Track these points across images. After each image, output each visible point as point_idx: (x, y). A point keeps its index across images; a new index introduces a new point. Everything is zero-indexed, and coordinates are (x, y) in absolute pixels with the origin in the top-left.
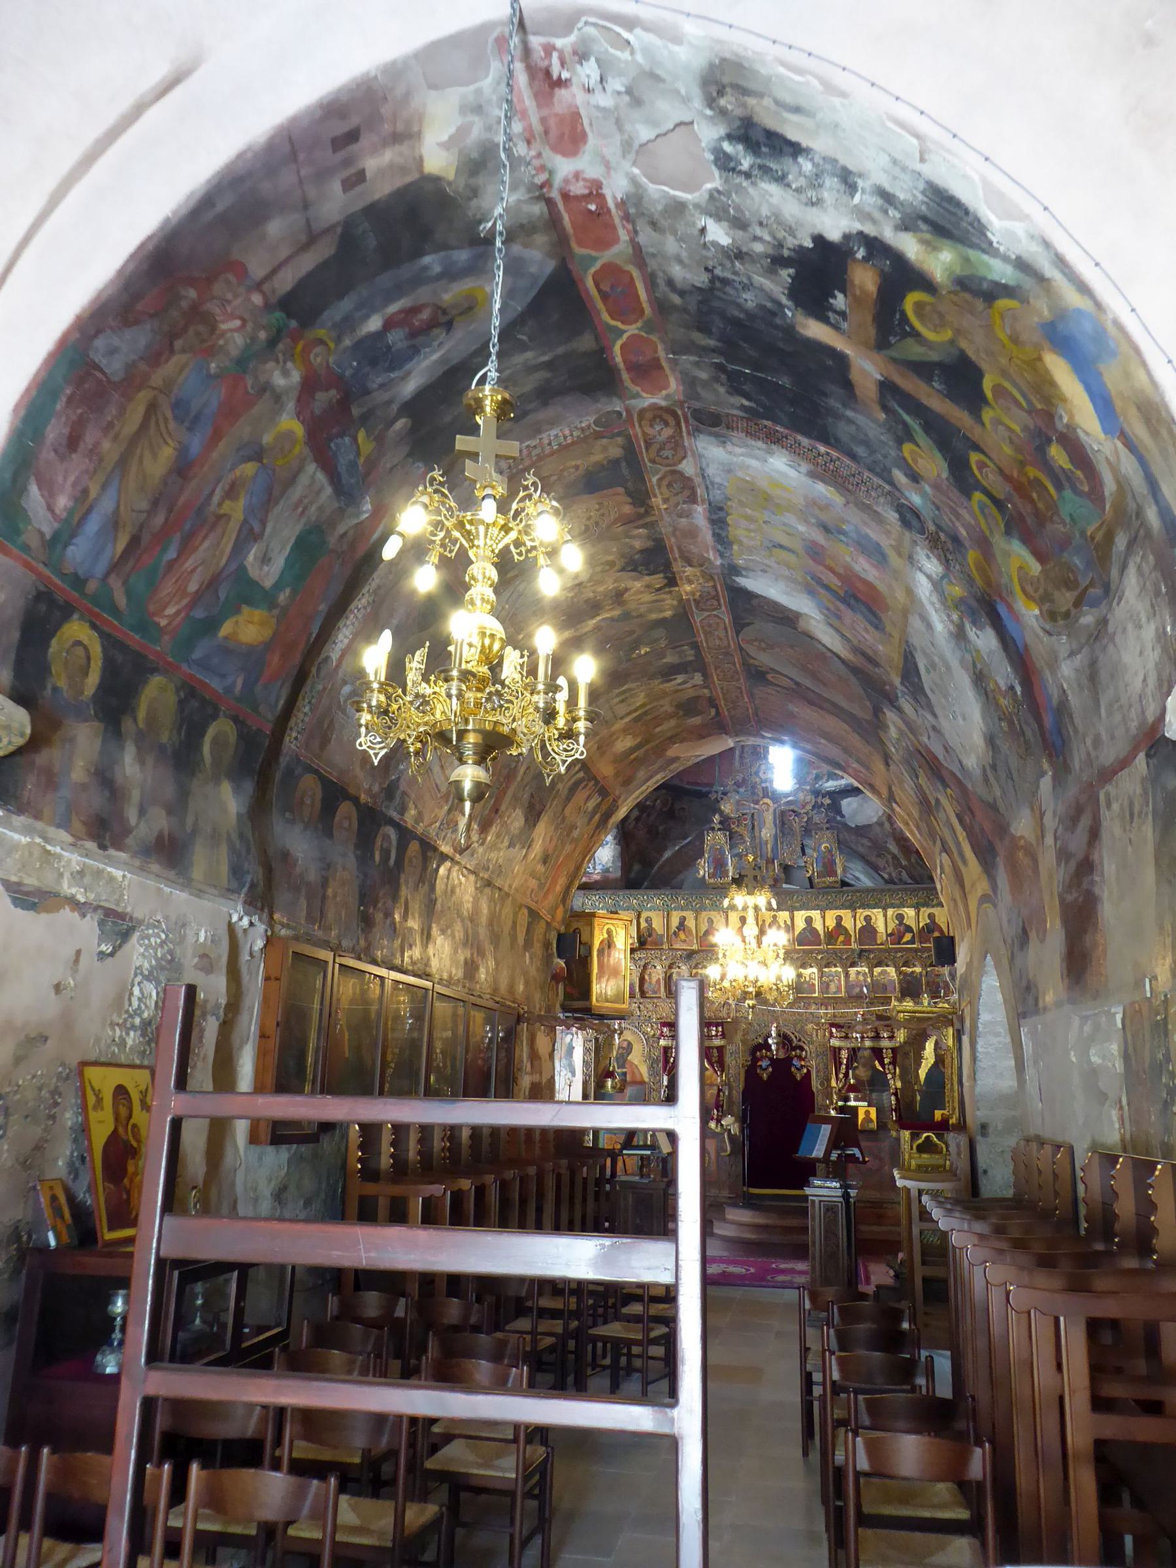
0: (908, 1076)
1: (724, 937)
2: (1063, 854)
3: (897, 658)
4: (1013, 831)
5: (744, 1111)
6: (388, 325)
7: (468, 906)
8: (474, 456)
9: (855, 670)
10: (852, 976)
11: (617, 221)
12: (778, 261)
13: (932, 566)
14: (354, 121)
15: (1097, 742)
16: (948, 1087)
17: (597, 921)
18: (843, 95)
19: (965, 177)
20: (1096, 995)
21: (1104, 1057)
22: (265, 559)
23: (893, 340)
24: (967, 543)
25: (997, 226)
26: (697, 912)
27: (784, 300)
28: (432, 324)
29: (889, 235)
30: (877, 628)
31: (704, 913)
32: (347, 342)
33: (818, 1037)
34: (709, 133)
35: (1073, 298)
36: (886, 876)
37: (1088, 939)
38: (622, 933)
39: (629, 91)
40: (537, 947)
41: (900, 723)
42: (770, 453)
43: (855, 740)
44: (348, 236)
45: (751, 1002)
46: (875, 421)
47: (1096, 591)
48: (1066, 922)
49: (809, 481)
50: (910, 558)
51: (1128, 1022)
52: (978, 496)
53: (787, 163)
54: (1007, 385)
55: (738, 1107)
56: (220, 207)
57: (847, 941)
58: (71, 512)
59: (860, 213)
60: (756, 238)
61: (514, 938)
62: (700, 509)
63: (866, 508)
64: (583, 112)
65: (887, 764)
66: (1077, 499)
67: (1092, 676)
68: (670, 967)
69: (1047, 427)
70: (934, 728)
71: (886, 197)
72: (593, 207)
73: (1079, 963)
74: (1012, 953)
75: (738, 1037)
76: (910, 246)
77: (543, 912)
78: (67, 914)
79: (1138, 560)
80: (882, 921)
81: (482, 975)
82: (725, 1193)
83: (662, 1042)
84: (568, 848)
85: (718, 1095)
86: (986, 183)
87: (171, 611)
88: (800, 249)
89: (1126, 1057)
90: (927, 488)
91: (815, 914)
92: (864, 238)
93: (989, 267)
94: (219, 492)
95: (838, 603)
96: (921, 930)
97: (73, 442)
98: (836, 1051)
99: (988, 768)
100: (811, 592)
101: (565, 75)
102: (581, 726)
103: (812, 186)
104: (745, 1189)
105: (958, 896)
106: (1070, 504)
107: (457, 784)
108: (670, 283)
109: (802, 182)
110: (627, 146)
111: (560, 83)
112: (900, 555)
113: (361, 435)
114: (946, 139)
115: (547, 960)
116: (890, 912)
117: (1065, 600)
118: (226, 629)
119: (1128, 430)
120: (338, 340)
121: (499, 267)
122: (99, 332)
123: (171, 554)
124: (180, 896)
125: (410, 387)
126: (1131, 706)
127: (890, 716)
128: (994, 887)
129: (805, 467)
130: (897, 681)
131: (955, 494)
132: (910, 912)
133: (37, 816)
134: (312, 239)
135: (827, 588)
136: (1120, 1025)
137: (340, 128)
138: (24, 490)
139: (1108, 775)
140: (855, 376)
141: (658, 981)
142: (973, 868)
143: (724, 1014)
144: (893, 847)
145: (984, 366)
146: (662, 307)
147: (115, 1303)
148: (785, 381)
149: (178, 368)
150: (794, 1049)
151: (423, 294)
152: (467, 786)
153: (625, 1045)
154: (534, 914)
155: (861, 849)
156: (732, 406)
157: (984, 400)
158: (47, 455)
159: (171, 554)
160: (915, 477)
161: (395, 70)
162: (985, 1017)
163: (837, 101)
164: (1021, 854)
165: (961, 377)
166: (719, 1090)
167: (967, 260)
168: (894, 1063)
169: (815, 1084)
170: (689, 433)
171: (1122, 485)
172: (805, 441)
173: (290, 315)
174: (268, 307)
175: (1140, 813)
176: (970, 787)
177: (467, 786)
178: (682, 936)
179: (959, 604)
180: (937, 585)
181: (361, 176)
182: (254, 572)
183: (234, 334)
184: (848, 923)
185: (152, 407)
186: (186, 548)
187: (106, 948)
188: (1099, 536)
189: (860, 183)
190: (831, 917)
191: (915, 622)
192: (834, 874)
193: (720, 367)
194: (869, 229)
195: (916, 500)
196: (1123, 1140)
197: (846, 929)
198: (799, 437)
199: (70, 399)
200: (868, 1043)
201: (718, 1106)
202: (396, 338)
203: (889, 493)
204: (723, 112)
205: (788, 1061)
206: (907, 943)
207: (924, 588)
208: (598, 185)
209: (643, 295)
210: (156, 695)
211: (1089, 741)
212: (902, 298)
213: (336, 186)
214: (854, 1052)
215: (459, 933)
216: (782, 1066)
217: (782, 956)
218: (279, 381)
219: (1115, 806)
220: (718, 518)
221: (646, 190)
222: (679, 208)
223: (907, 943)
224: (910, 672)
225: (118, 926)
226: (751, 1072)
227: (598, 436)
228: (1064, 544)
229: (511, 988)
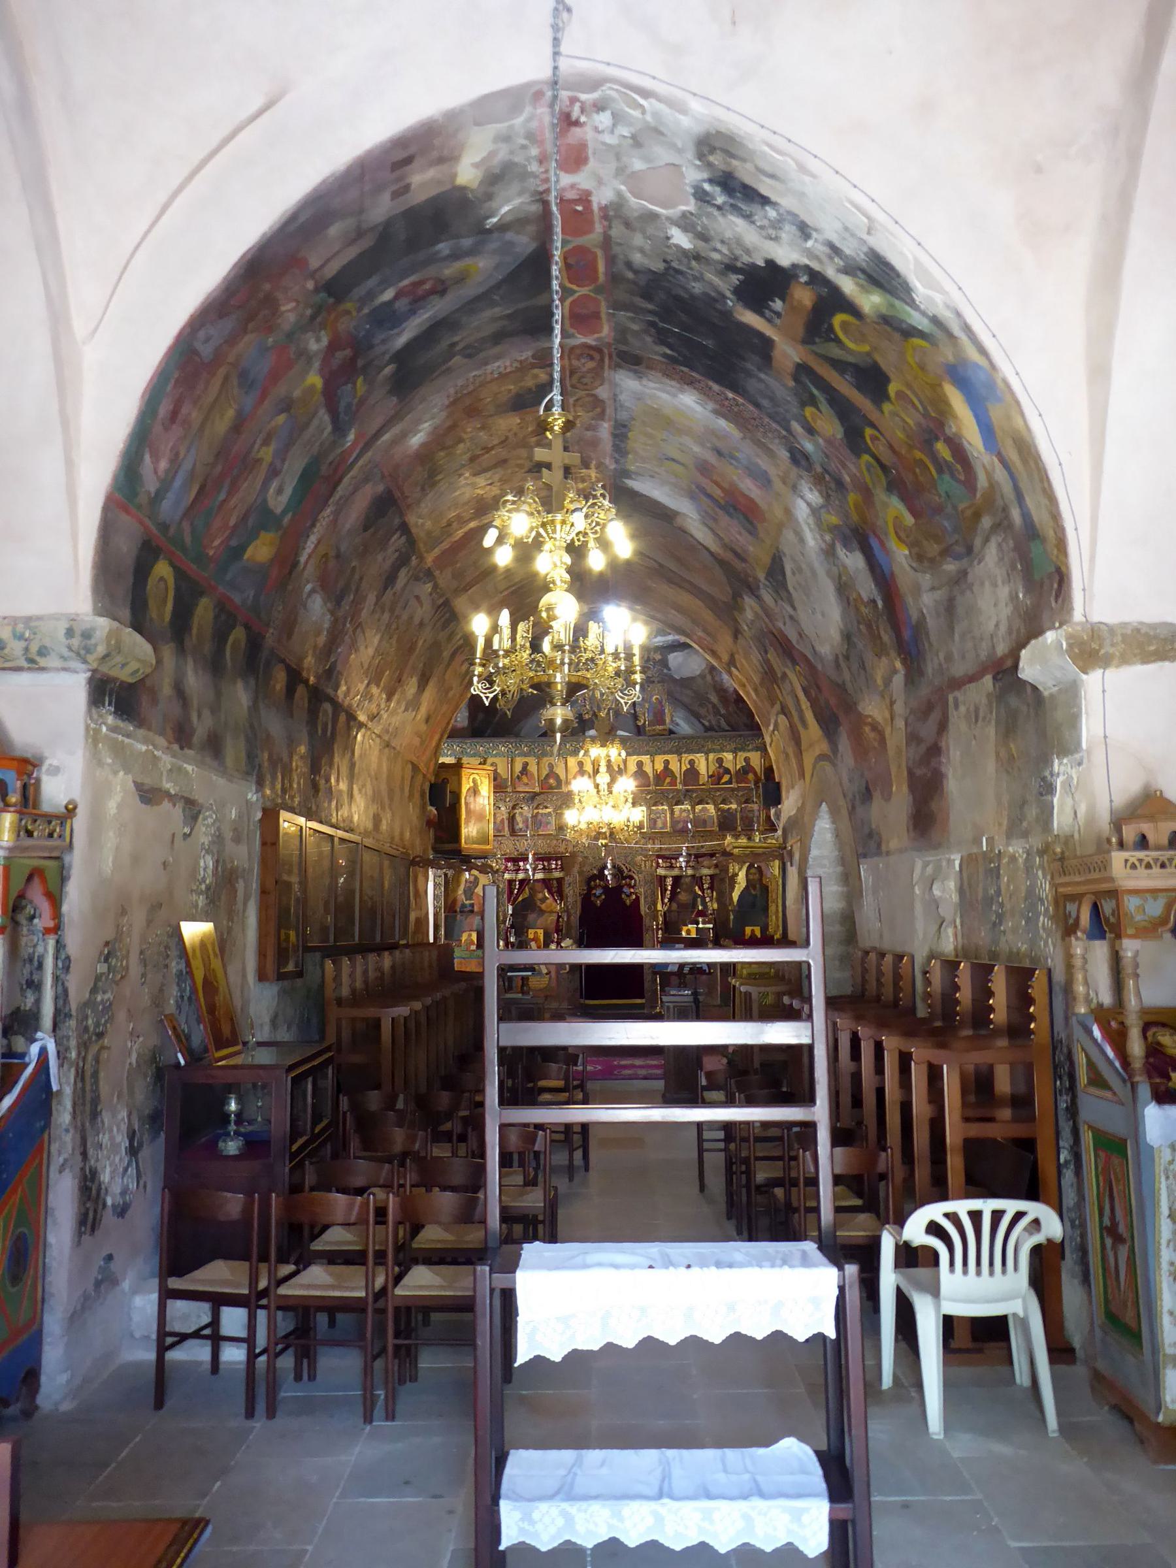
0: (724, 898)
1: (580, 785)
2: (913, 738)
3: (766, 560)
4: (860, 709)
5: (582, 935)
7: (374, 766)
8: (549, 466)
9: (722, 563)
10: (677, 813)
11: (596, 218)
12: (730, 267)
13: (814, 497)
14: (412, 150)
15: (949, 658)
16: (772, 908)
17: (464, 772)
18: (814, 176)
19: (901, 253)
20: (937, 846)
21: (943, 891)
22: (280, 491)
23: (817, 340)
24: (850, 487)
25: (921, 291)
26: (539, 759)
27: (728, 294)
28: (432, 292)
29: (830, 272)
30: (751, 533)
31: (545, 759)
32: (366, 311)
33: (646, 866)
34: (694, 175)
35: (973, 355)
36: (707, 724)
37: (934, 805)
38: (486, 781)
39: (634, 137)
40: (417, 795)
41: (758, 608)
42: (682, 391)
43: (708, 616)
44: (385, 233)
45: (604, 842)
46: (784, 385)
47: (959, 549)
48: (912, 788)
49: (712, 416)
50: (794, 488)
51: (964, 867)
52: (866, 457)
53: (755, 208)
54: (908, 392)
55: (575, 932)
56: (302, 219)
57: (673, 783)
58: (167, 471)
59: (809, 253)
60: (715, 250)
61: (402, 790)
62: (606, 425)
63: (759, 444)
64: (591, 145)
65: (736, 637)
66: (954, 483)
67: (949, 608)
68: (514, 808)
69: (935, 426)
70: (791, 617)
71: (835, 250)
72: (579, 208)
73: (926, 820)
74: (854, 807)
75: (576, 869)
76: (847, 285)
77: (422, 766)
78: (166, 805)
79: (1000, 539)
80: (703, 764)
81: (384, 826)
82: (565, 1005)
83: (507, 876)
84: (445, 708)
85: (558, 921)
86: (916, 260)
87: (216, 543)
88: (754, 266)
89: (961, 891)
90: (821, 441)
91: (646, 759)
92: (808, 270)
93: (910, 315)
94: (259, 442)
95: (718, 510)
96: (737, 772)
97: (174, 415)
98: (662, 879)
99: (841, 657)
100: (692, 497)
101: (583, 119)
102: (638, 677)
103: (775, 228)
104: (582, 1001)
105: (790, 751)
106: (946, 483)
107: (551, 722)
108: (629, 265)
109: (766, 222)
110: (620, 171)
111: (577, 123)
112: (784, 483)
113: (360, 380)
114: (891, 226)
115: (423, 807)
116: (711, 756)
117: (933, 549)
119: (1004, 453)
120: (359, 310)
121: (557, 307)
122: (202, 325)
123: (222, 496)
124: (221, 781)
125: (402, 340)
126: (982, 639)
127: (749, 602)
128: (835, 750)
129: (711, 405)
130: (761, 576)
131: (847, 452)
132: (728, 756)
133: (149, 729)
134: (360, 234)
135: (710, 496)
136: (957, 868)
137: (401, 155)
138: (142, 459)
139: (957, 684)
140: (776, 354)
141: (502, 821)
142: (813, 730)
143: (562, 850)
144: (714, 698)
145: (892, 376)
146: (615, 279)
147: (229, 1104)
148: (709, 343)
149: (248, 344)
150: (625, 878)
151: (431, 271)
152: (559, 721)
153: (472, 879)
154: (415, 768)
155: (686, 700)
156: (656, 353)
157: (888, 398)
158: (158, 428)
159: (222, 496)
160: (811, 431)
161: (452, 116)
162: (814, 852)
163: (807, 179)
164: (867, 729)
165: (873, 379)
166: (559, 917)
167: (892, 306)
168: (711, 888)
169: (644, 909)
170: (610, 367)
171: (993, 486)
172: (716, 387)
173: (330, 295)
174: (317, 290)
175: (984, 718)
176: (819, 667)
177: (559, 721)
178: (525, 779)
179: (832, 529)
180: (815, 511)
181: (407, 188)
182: (271, 503)
183: (289, 313)
184: (674, 766)
185: (226, 378)
186: (234, 488)
187: (187, 830)
188: (969, 513)
189: (814, 234)
190: (659, 761)
191: (789, 535)
192: (663, 722)
193: (652, 324)
194: (815, 266)
195: (809, 447)
196: (956, 949)
197: (672, 772)
198: (711, 383)
199: (177, 381)
200: (690, 872)
201: (558, 930)
202: (402, 305)
203: (785, 437)
204: (710, 165)
205: (618, 889)
206: (726, 783)
207: (802, 511)
208: (588, 193)
209: (601, 268)
210: (204, 612)
211: (942, 656)
212: (832, 315)
213: (386, 197)
214: (677, 880)
215: (369, 789)
216: (614, 894)
217: (630, 800)
218: (314, 346)
219: (962, 709)
220: (621, 433)
221: (627, 201)
222: (654, 216)
223: (726, 783)
224: (776, 571)
225: (192, 809)
226: (587, 899)
227: (533, 366)
228: (939, 510)
229: (402, 834)
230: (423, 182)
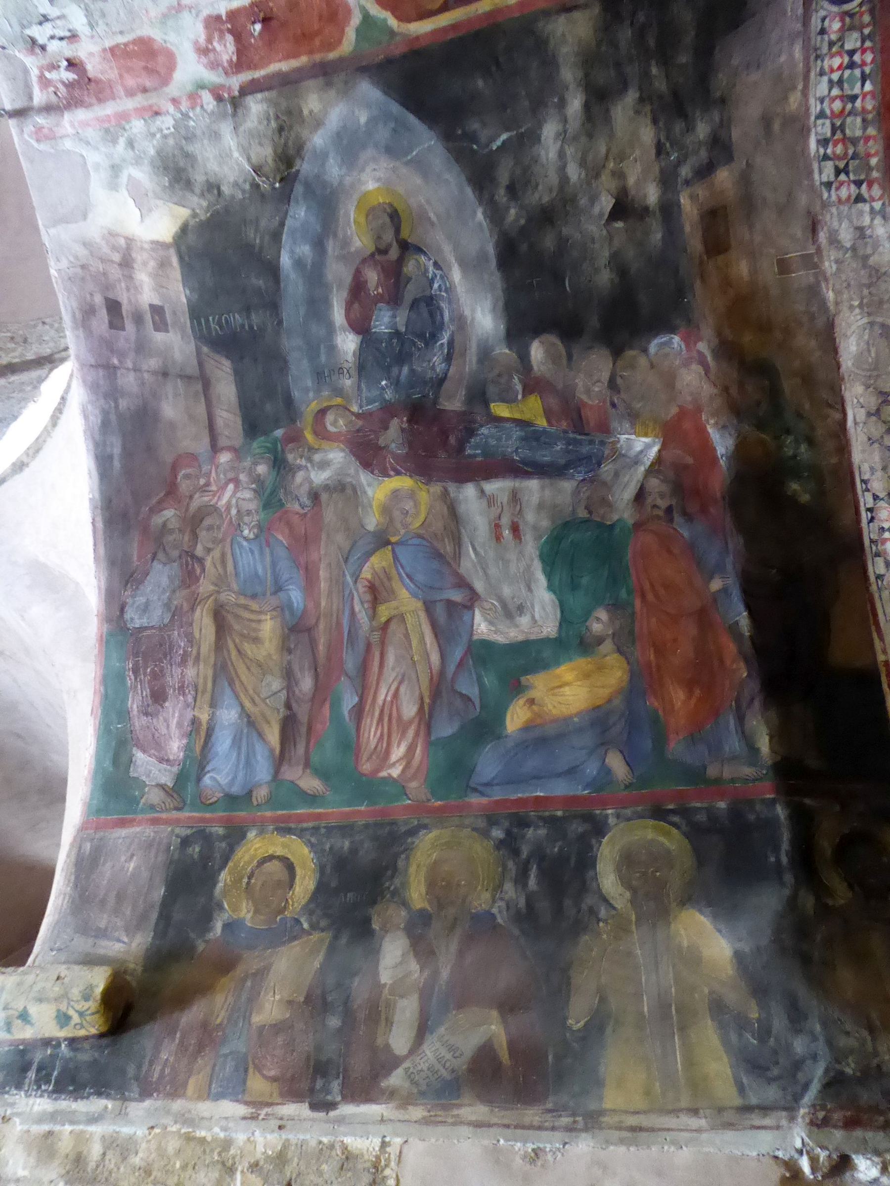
6: (360, 326)
14: (98, 299)
32: (348, 383)
64: (108, 44)
87: (398, 752)
118: (516, 718)
123: (349, 701)
158: (139, 722)
181: (157, 310)
230: (155, 286)
